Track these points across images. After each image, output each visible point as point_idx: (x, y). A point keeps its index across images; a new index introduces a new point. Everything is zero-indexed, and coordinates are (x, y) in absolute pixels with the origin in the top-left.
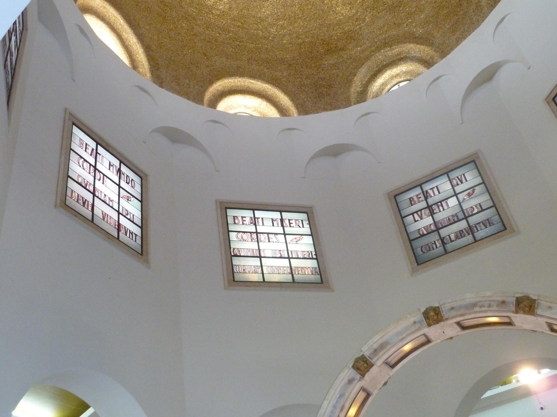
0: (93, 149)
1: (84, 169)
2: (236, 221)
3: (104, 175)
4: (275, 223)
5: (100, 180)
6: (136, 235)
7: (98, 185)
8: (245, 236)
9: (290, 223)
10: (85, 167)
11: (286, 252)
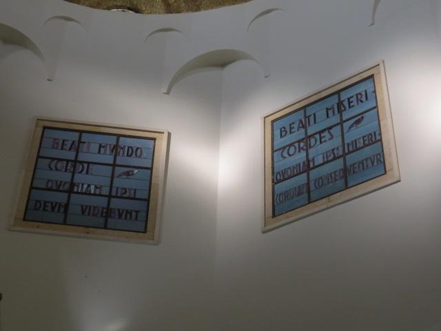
0: (74, 142)
1: (57, 170)
2: (284, 133)
3: (89, 163)
4: (330, 112)
5: (82, 171)
6: (137, 212)
7: (79, 178)
8: (292, 150)
9: (349, 103)
10: (58, 168)
11: (341, 149)
